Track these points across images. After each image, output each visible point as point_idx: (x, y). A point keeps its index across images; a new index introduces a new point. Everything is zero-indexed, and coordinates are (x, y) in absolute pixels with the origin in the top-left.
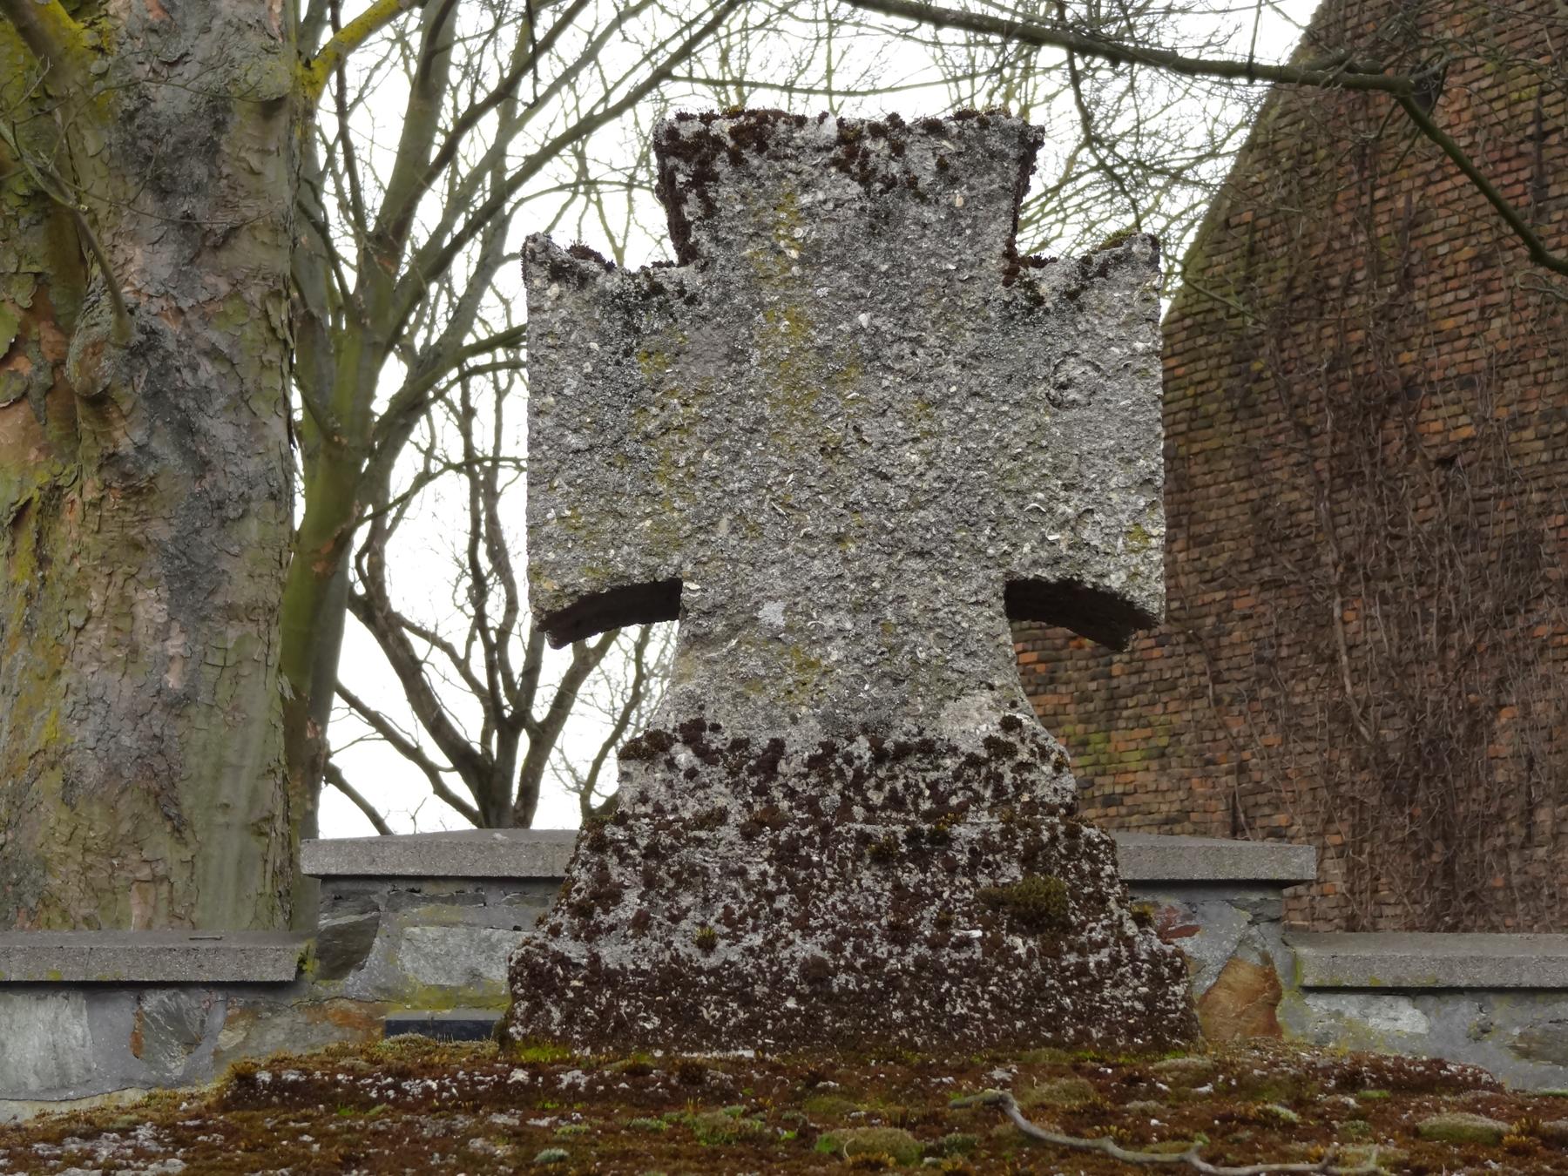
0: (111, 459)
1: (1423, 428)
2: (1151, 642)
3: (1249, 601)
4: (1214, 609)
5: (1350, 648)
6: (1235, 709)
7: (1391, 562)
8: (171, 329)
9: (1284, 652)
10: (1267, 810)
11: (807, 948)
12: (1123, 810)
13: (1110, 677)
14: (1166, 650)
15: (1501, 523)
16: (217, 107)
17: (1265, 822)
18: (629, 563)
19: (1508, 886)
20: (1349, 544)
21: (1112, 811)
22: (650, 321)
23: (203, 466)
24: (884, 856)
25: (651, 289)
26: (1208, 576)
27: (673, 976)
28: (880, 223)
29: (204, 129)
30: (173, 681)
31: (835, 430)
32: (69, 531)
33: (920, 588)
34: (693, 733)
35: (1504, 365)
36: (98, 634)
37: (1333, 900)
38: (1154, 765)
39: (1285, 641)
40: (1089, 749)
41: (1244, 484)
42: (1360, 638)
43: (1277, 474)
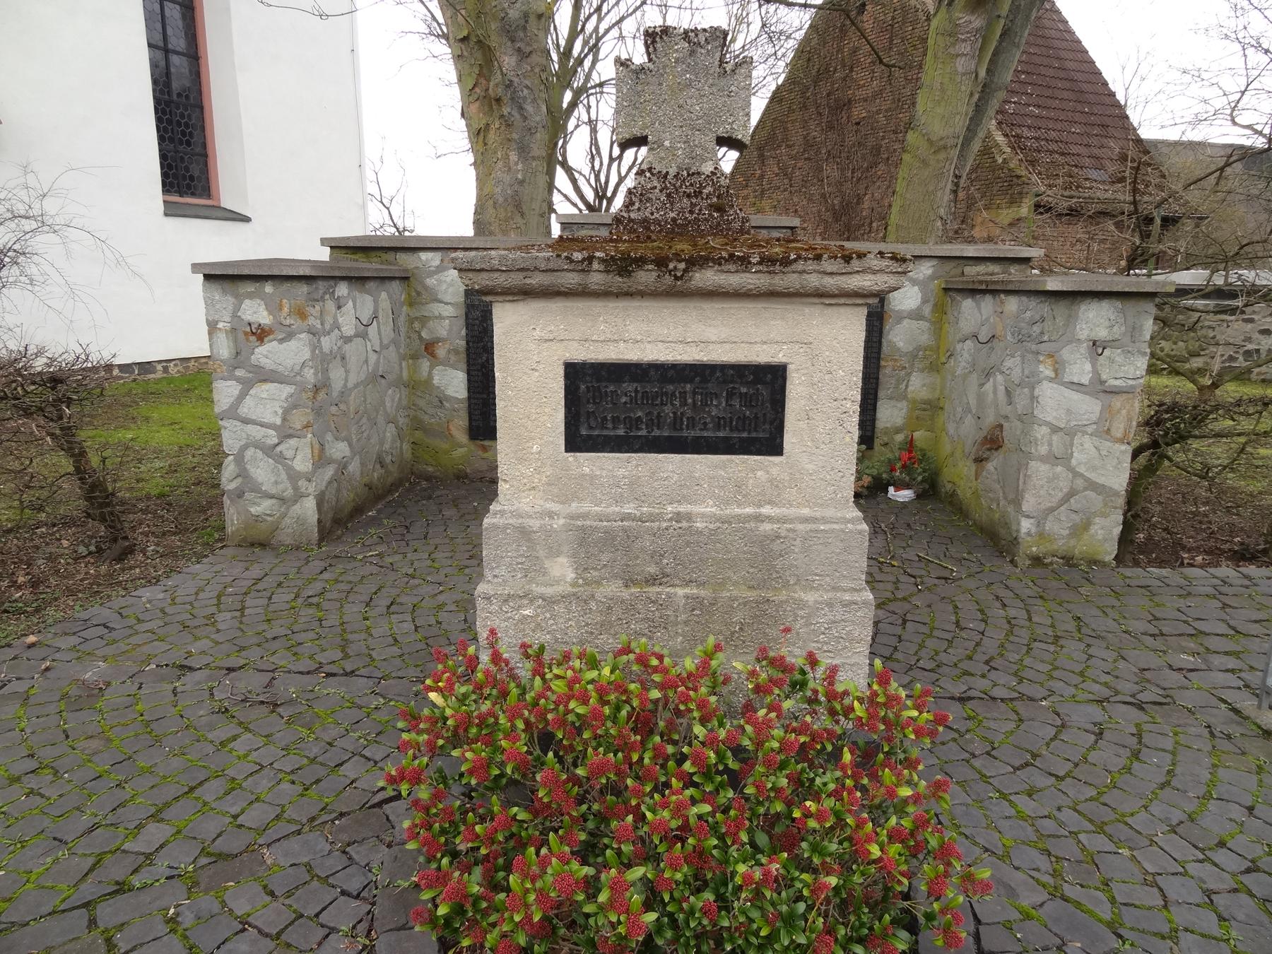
0: (502, 116)
8: (516, 80)
11: (672, 215)
15: (871, 142)
16: (526, 16)
18: (637, 132)
22: (642, 76)
23: (525, 118)
24: (689, 196)
25: (642, 69)
27: (645, 220)
28: (692, 53)
29: (522, 22)
30: (520, 176)
31: (681, 102)
32: (492, 135)
33: (698, 138)
34: (650, 169)
35: (876, 95)
36: (500, 164)
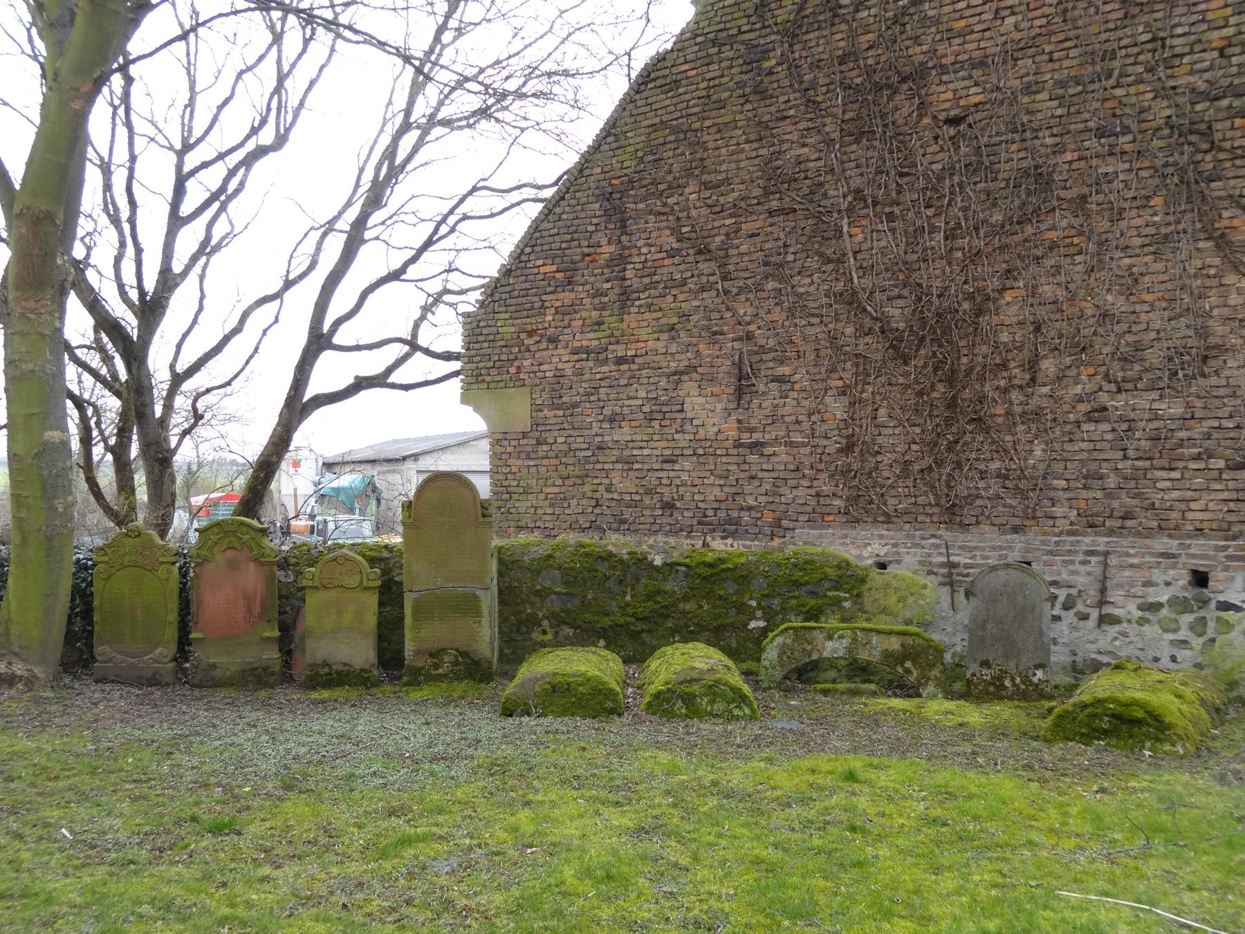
1: (934, 98)
2: (664, 255)
3: (759, 224)
4: (722, 231)
5: (855, 253)
6: (742, 298)
7: (899, 193)
9: (790, 258)
10: (771, 365)
12: (634, 367)
13: (624, 279)
14: (677, 260)
15: (1011, 160)
17: (769, 372)
19: (1009, 413)
20: (857, 182)
21: (624, 367)
26: (718, 209)
35: (1011, 55)
37: (831, 424)
38: (665, 336)
39: (791, 250)
40: (603, 327)
41: (755, 145)
42: (864, 246)
43: (788, 137)
